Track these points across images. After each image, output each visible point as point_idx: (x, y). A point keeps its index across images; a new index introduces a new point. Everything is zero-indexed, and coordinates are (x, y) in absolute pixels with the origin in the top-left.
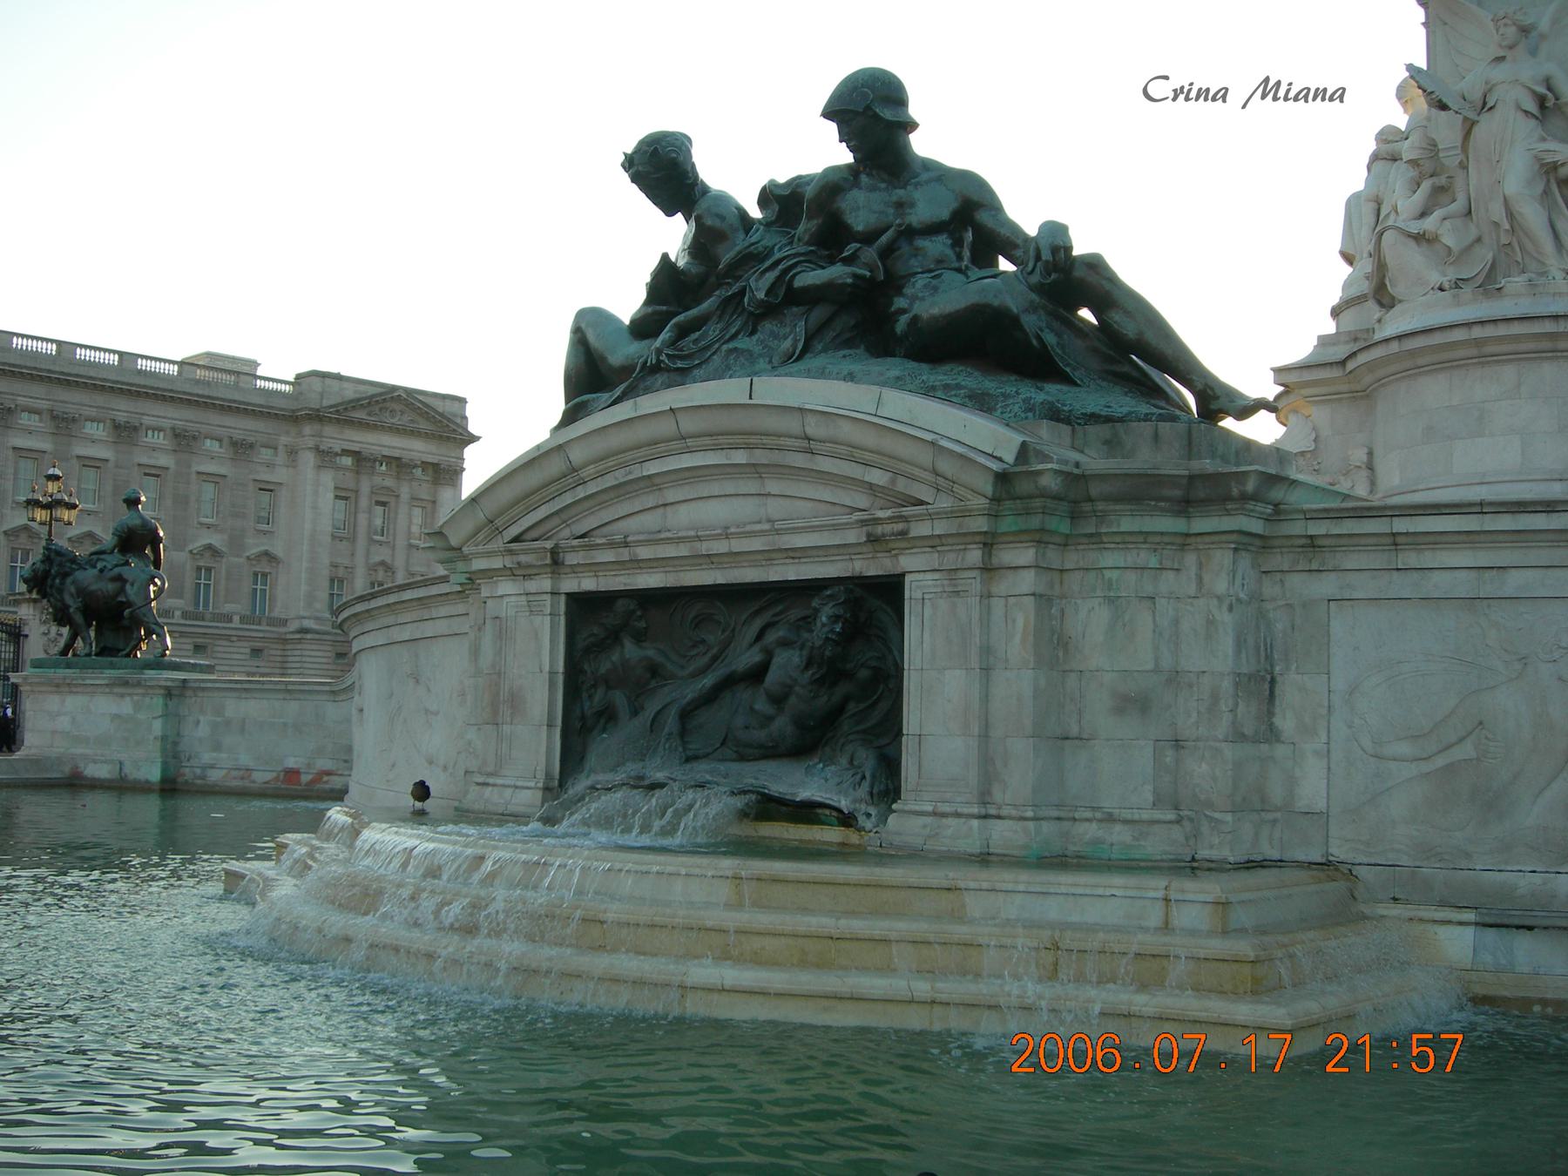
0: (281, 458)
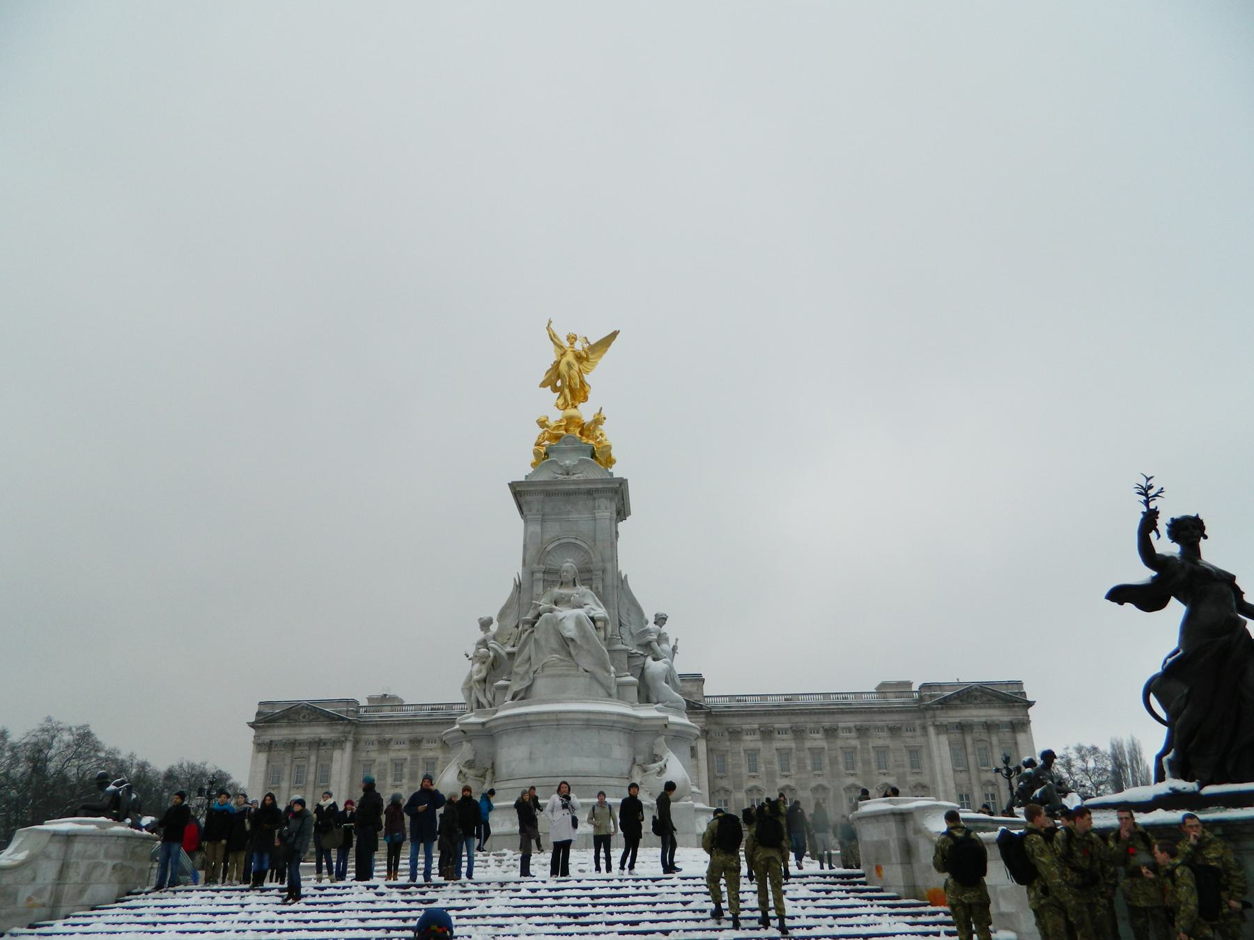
0: (919, 732)
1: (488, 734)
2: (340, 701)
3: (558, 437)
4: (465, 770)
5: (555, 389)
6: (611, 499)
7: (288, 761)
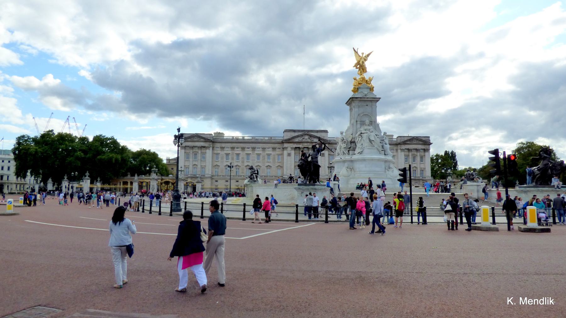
1: (352, 161)
3: (359, 84)
5: (357, 68)
7: (191, 152)
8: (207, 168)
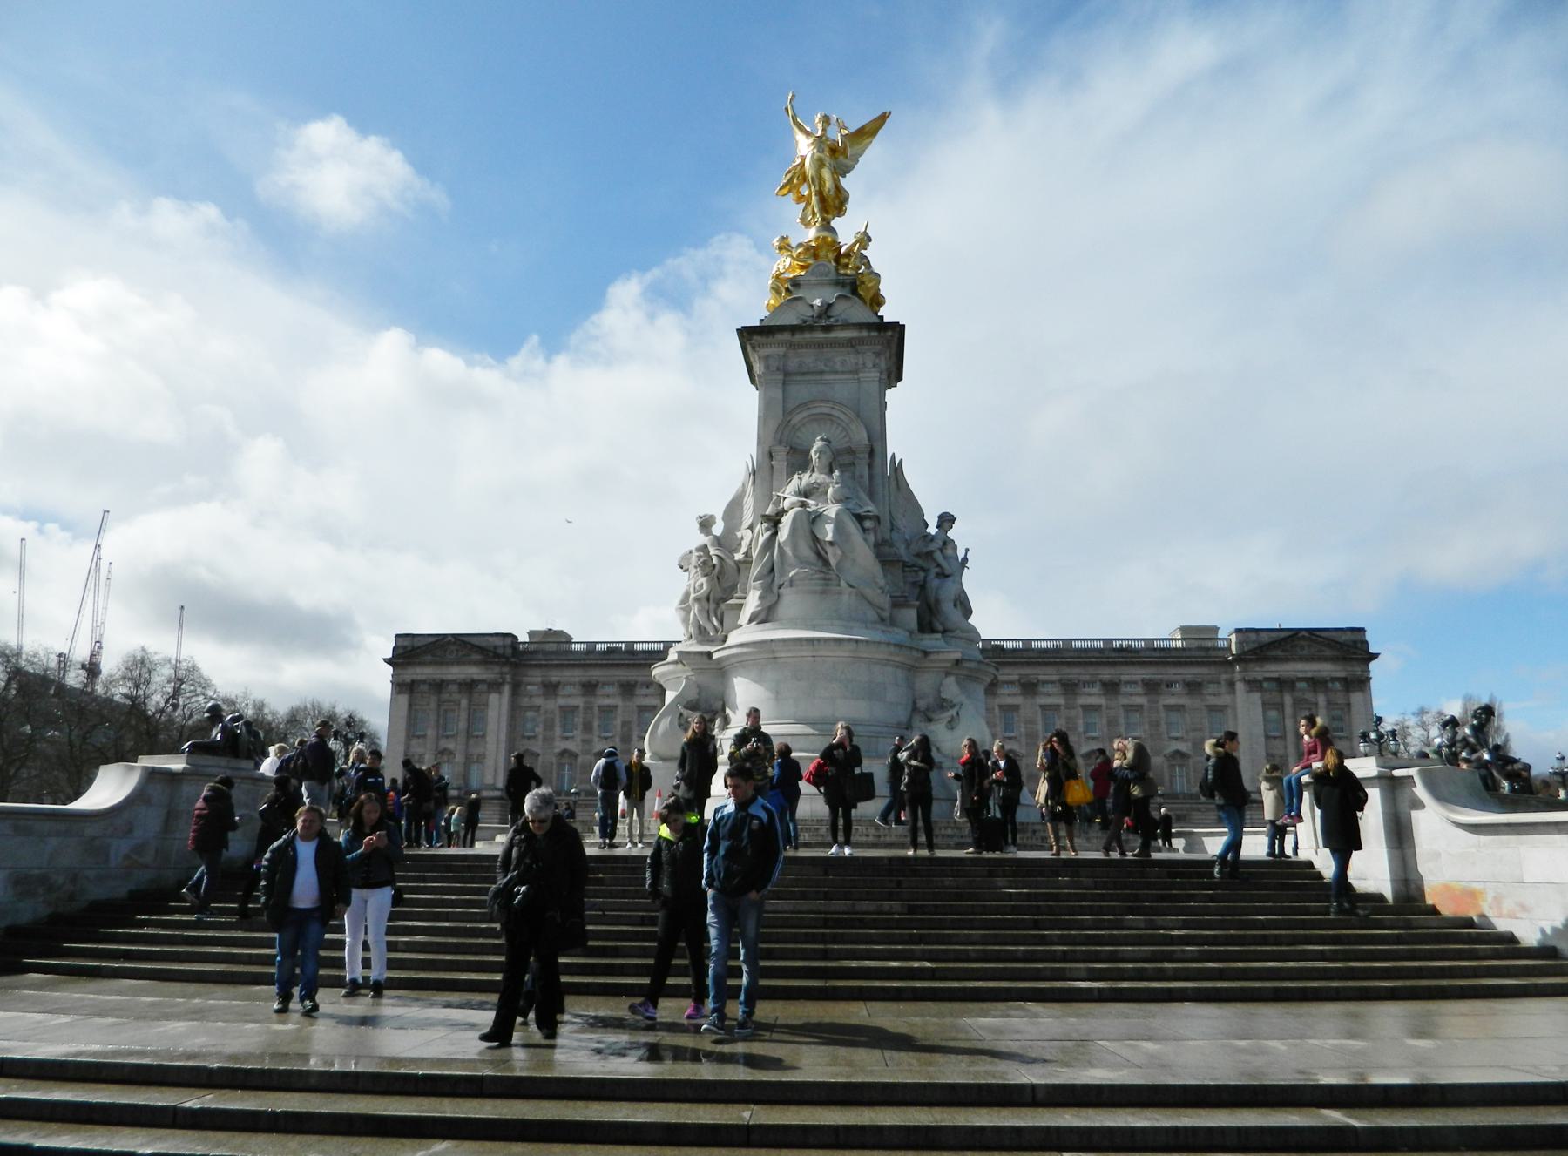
0: (1223, 689)
2: (497, 635)
4: (686, 712)
5: (800, 198)
6: (878, 354)
7: (433, 705)
8: (489, 762)
